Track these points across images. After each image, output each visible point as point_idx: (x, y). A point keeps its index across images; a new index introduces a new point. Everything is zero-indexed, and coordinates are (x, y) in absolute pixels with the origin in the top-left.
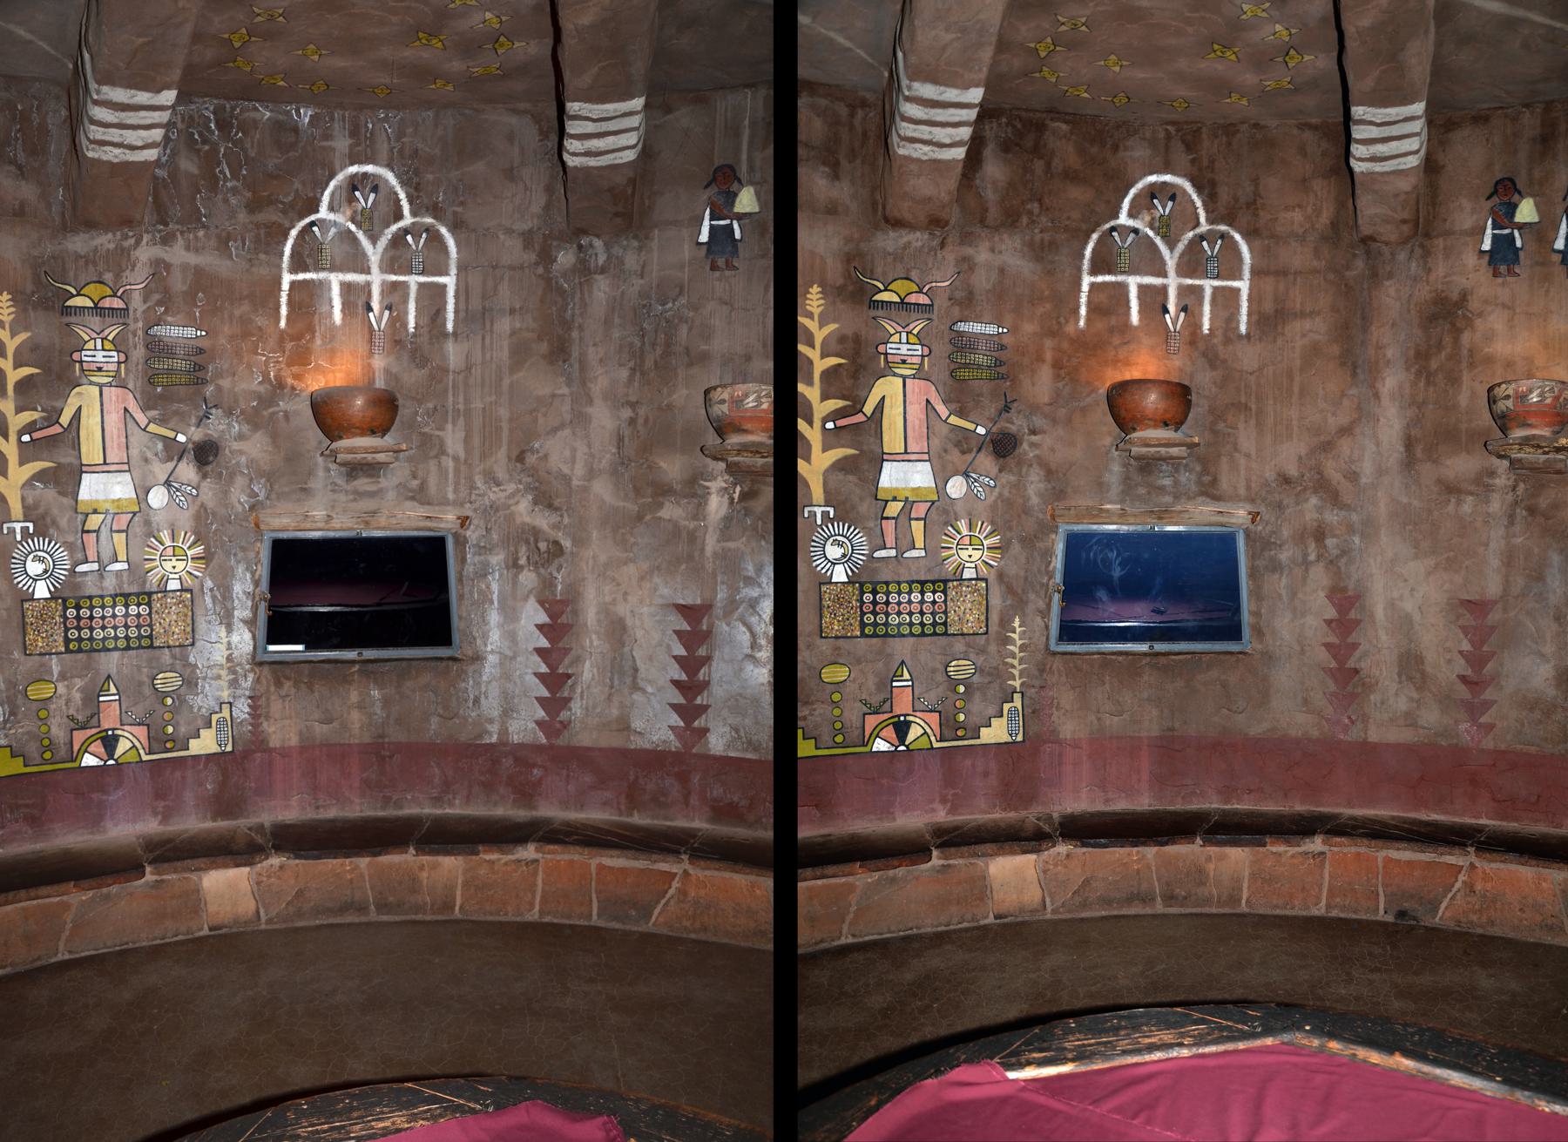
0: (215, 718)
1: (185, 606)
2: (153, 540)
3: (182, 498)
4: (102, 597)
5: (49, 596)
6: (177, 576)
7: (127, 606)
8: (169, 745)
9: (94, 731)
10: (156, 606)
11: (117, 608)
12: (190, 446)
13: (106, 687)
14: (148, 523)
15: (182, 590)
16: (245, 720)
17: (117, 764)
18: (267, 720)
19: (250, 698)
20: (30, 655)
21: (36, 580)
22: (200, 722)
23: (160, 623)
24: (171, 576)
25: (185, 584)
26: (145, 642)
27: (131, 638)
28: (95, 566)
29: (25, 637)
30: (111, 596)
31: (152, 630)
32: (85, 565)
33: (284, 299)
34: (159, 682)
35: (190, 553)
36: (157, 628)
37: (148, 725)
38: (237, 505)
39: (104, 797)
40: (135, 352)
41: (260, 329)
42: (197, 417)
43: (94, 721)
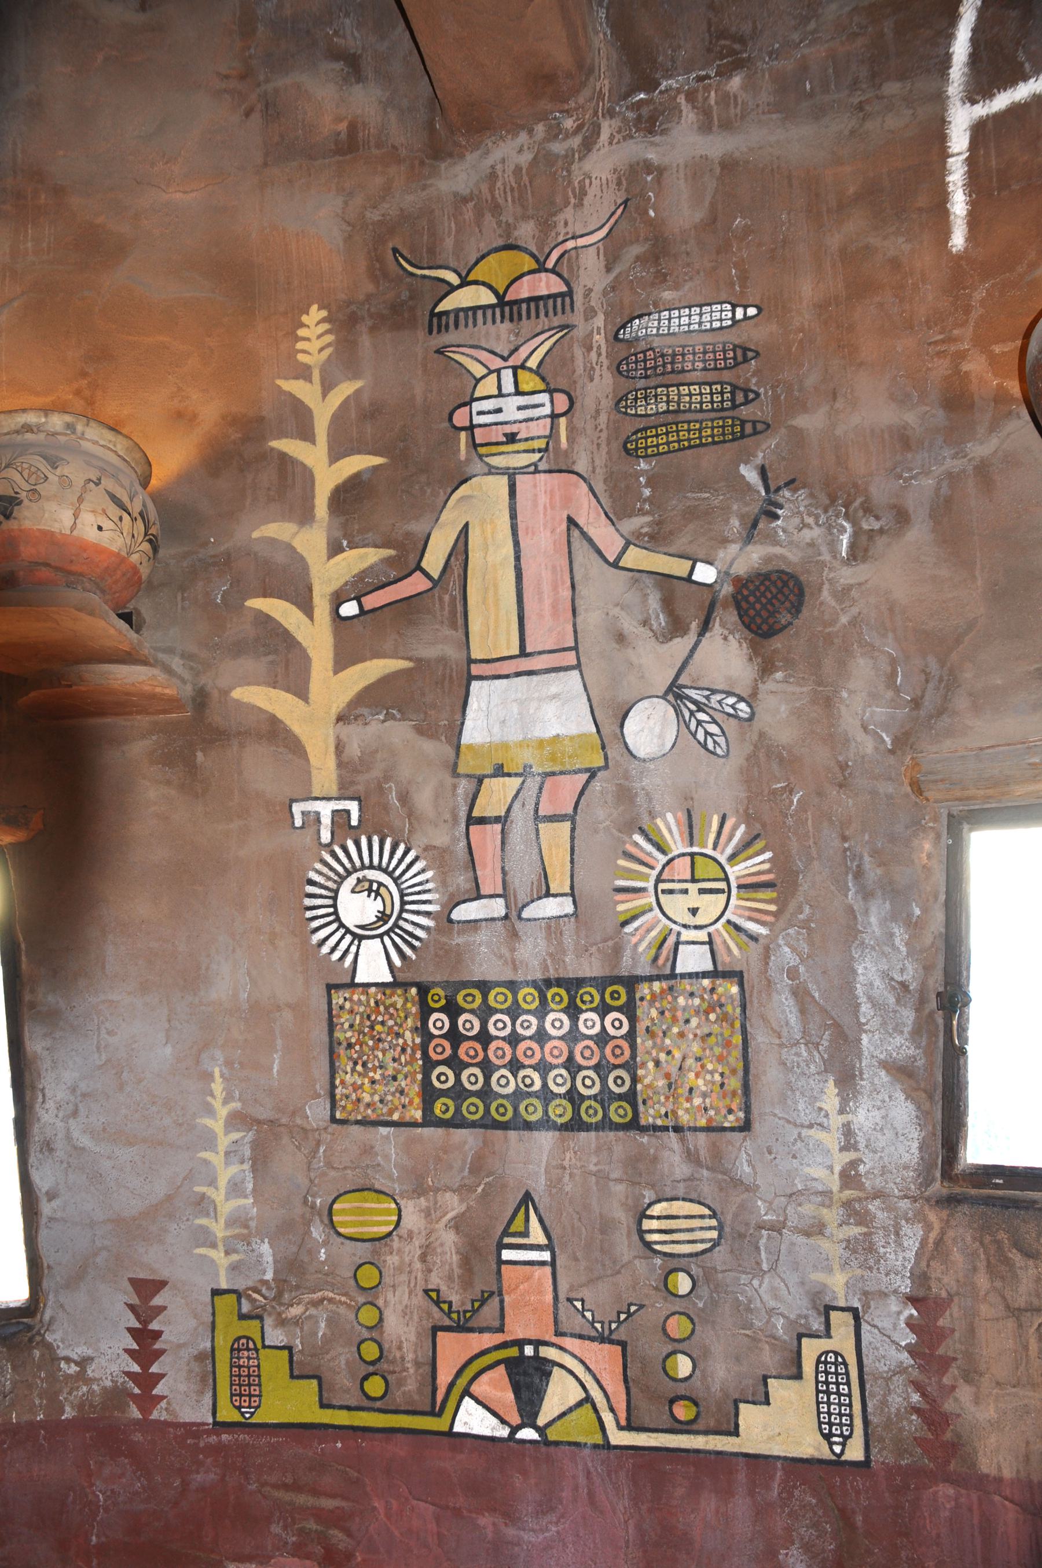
0: (811, 1349)
1: (724, 1018)
2: (638, 838)
3: (713, 729)
4: (512, 986)
5: (388, 978)
6: (702, 935)
7: (573, 1011)
8: (683, 1412)
9: (488, 1340)
10: (648, 1014)
11: (551, 1016)
12: (727, 589)
13: (518, 1225)
14: (625, 795)
15: (714, 974)
16: (901, 1370)
17: (546, 1442)
18: (968, 1381)
19: (913, 1300)
20: (343, 1122)
21: (361, 938)
22: (769, 1359)
23: (657, 1063)
24: (687, 935)
25: (723, 957)
26: (619, 1112)
27: (583, 1098)
28: (497, 908)
29: (332, 1078)
30: (534, 984)
31: (635, 1080)
32: (475, 904)
33: (956, 175)
34: (654, 1224)
35: (735, 872)
36: (648, 1074)
37: (623, 1344)
38: (860, 736)
39: (511, 1532)
40: (590, 387)
41: (895, 264)
42: (742, 517)
43: (489, 1313)
